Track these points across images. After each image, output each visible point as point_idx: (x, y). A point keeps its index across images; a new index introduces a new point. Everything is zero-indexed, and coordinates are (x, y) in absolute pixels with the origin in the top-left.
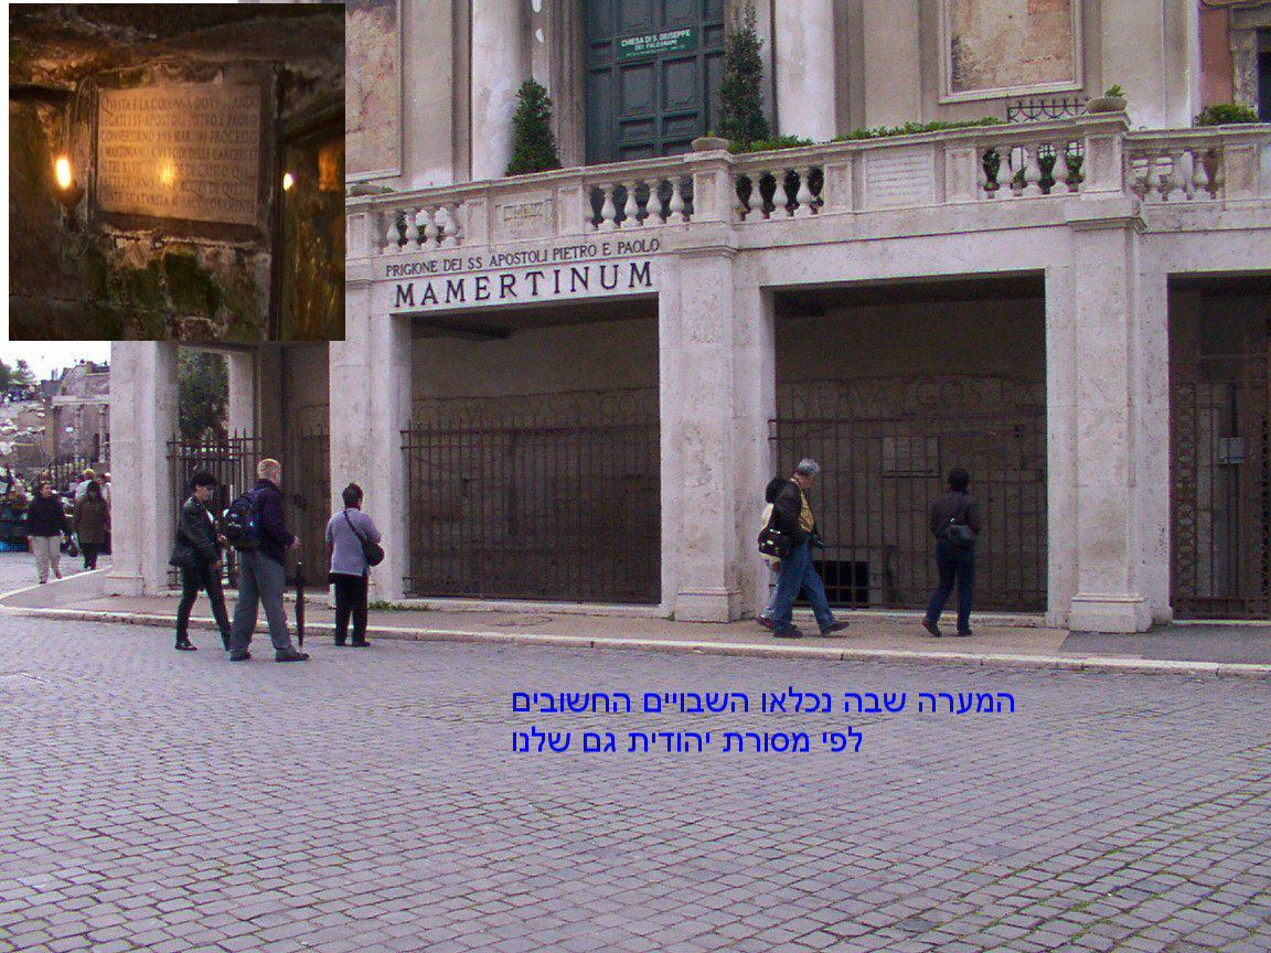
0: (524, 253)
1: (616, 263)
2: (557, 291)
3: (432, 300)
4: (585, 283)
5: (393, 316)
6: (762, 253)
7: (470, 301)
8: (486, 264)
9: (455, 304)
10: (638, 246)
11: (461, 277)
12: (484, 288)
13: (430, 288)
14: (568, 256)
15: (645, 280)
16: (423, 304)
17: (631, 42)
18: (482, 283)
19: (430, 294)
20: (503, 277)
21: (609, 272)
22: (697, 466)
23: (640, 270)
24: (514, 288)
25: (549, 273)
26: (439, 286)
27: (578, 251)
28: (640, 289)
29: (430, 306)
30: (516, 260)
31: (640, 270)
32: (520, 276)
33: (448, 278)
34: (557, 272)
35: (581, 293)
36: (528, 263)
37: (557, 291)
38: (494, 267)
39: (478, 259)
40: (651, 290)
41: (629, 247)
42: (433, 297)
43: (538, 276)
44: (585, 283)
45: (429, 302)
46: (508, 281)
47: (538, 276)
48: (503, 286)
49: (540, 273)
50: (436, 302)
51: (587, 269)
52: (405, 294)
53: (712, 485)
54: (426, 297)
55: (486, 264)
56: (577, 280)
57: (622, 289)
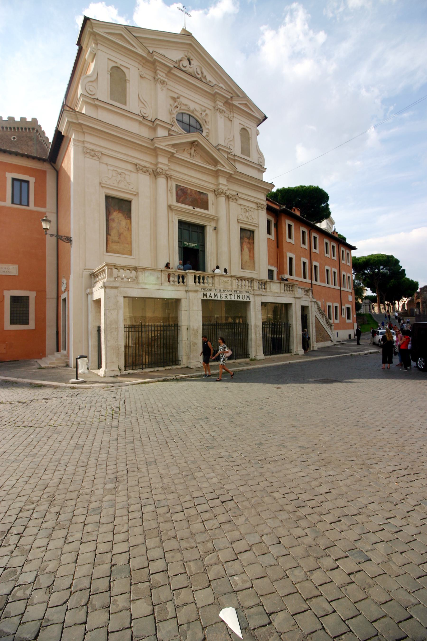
5: (202, 300)
7: (219, 299)
8: (222, 291)
9: (216, 299)
17: (186, 243)
19: (211, 296)
25: (233, 295)
28: (248, 300)
29: (210, 298)
32: (228, 294)
35: (239, 300)
45: (210, 297)
52: (205, 295)
55: (222, 291)
57: (245, 300)
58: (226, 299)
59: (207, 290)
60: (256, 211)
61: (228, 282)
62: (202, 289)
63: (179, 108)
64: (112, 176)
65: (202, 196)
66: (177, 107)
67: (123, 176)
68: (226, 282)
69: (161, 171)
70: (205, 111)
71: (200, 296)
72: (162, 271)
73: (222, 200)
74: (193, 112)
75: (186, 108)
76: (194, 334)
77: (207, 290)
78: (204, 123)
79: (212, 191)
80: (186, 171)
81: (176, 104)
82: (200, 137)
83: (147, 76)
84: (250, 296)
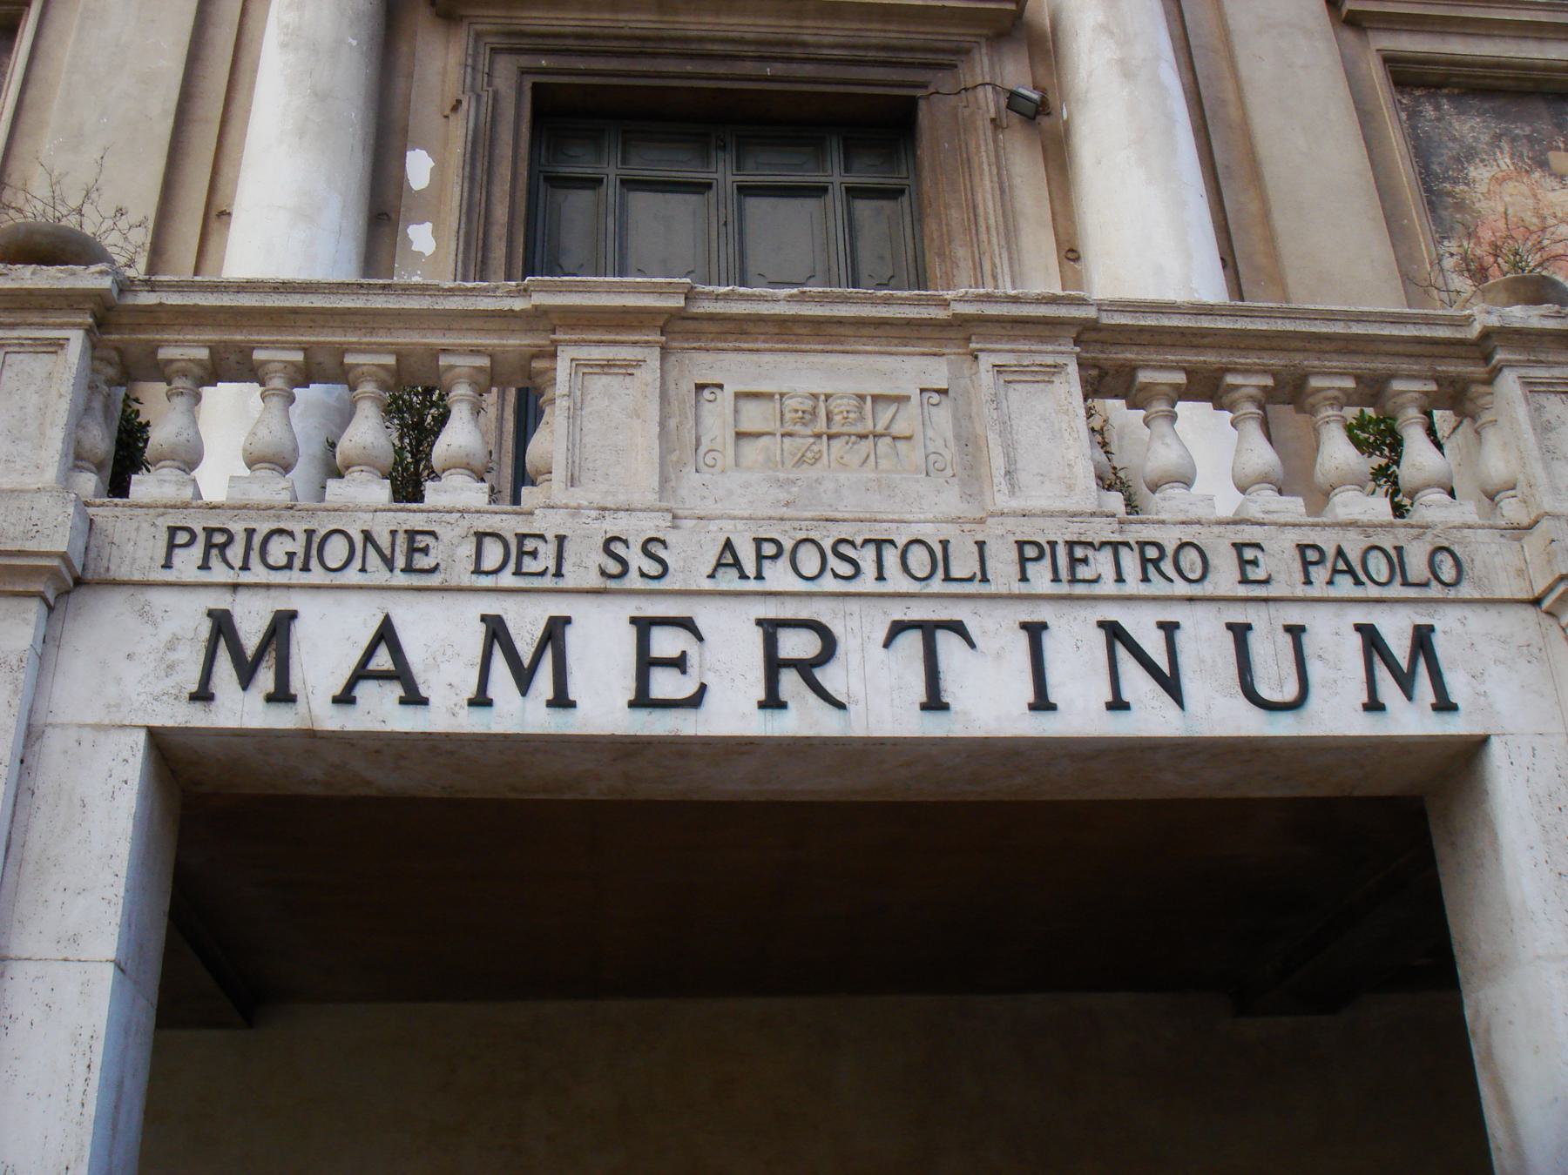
0: (879, 544)
1: (1294, 615)
2: (1042, 703)
3: (396, 690)
4: (1171, 684)
7: (602, 705)
8: (691, 559)
9: (519, 713)
11: (558, 607)
13: (386, 634)
14: (1083, 572)
16: (345, 698)
18: (665, 643)
19: (385, 660)
20: (771, 628)
21: (1270, 654)
23: (1400, 648)
24: (823, 675)
25: (998, 630)
26: (442, 638)
27: (1130, 562)
28: (1410, 719)
29: (380, 710)
30: (833, 562)
31: (1400, 648)
32: (859, 630)
33: (492, 606)
34: (1035, 631)
35: (1152, 716)
36: (902, 584)
37: (1042, 703)
38: (729, 580)
39: (648, 547)
41: (1343, 566)
42: (401, 674)
43: (947, 643)
44: (1171, 684)
46: (797, 645)
47: (947, 643)
48: (774, 665)
49: (958, 628)
50: (413, 698)
54: (362, 673)
55: (691, 559)
56: (1129, 667)
57: (1336, 713)
58: (803, 718)
59: (316, 545)
84: (1449, 627)
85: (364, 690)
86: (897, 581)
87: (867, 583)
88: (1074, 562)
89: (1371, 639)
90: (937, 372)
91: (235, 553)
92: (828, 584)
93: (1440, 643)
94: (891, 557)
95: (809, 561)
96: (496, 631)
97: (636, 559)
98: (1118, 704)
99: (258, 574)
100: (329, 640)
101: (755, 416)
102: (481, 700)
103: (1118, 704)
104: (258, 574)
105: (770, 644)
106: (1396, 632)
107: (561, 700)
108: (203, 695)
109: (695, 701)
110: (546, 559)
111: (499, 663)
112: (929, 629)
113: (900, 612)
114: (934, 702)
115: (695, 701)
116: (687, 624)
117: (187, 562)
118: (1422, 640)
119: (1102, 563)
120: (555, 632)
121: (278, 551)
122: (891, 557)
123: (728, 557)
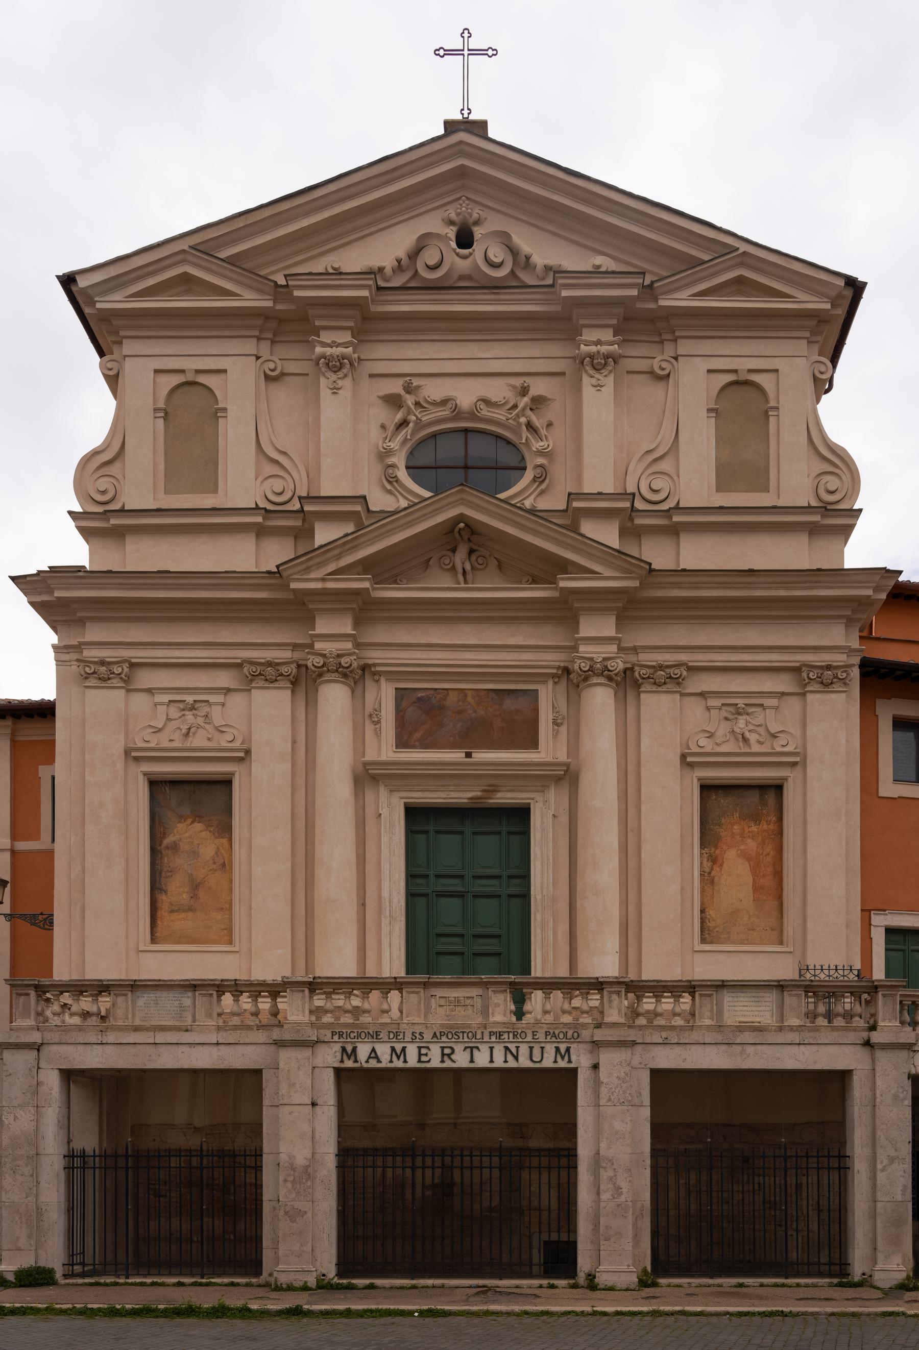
1: (543, 1045)
2: (492, 1061)
4: (516, 1058)
6: (651, 1047)
8: (428, 1036)
9: (399, 1064)
10: (561, 1036)
12: (426, 1055)
13: (373, 1050)
15: (566, 1058)
16: (367, 1062)
18: (424, 1051)
20: (443, 1048)
22: (610, 1186)
23: (563, 1051)
24: (453, 1057)
25: (485, 1048)
26: (384, 1050)
27: (511, 1035)
28: (562, 1064)
29: (373, 1064)
31: (563, 1051)
32: (458, 1048)
34: (491, 1048)
35: (512, 1064)
37: (492, 1061)
39: (421, 1034)
40: (571, 1065)
42: (377, 1057)
44: (516, 1058)
46: (447, 1051)
47: (475, 1051)
48: (443, 1055)
50: (379, 1061)
51: (517, 1047)
53: (623, 1198)
54: (369, 1057)
55: (428, 1036)
57: (548, 1062)
58: (448, 1064)
59: (359, 1036)
60: (794, 703)
61: (468, 1002)
62: (333, 1034)
63: (411, 425)
64: (169, 719)
65: (509, 704)
66: (404, 423)
67: (205, 709)
68: (457, 1003)
69: (319, 661)
70: (524, 391)
71: (330, 1056)
72: (195, 986)
73: (600, 700)
74: (472, 415)
75: (445, 412)
76: (293, 1182)
77: (359, 1036)
78: (525, 434)
79: (553, 676)
80: (437, 635)
81: (399, 416)
82: (470, 498)
83: (292, 367)
84: (574, 1047)
85: (370, 1060)
86: (466, 1039)
87: (461, 1040)
88: (500, 1035)
89: (557, 1049)
90: (480, 991)
91: (344, 1036)
92: (453, 1040)
93: (572, 1050)
94: (465, 1035)
95: (450, 1037)
96: (393, 1049)
97: (418, 1036)
98: (506, 1061)
99: (349, 1040)
100: (363, 1051)
101: (442, 1002)
102: (391, 1061)
103: (506, 1061)
104: (349, 1040)
105: (442, 1051)
106: (563, 1048)
107: (405, 1061)
108: (342, 1061)
109: (429, 1061)
110: (401, 1036)
111: (394, 1055)
112: (472, 1048)
113: (467, 1045)
114: (472, 1061)
115: (429, 1061)
116: (428, 1048)
117: (336, 1038)
118: (568, 1050)
119: (506, 1036)
120: (404, 1049)
121: (352, 1035)
122: (465, 1035)
123: (435, 1035)
